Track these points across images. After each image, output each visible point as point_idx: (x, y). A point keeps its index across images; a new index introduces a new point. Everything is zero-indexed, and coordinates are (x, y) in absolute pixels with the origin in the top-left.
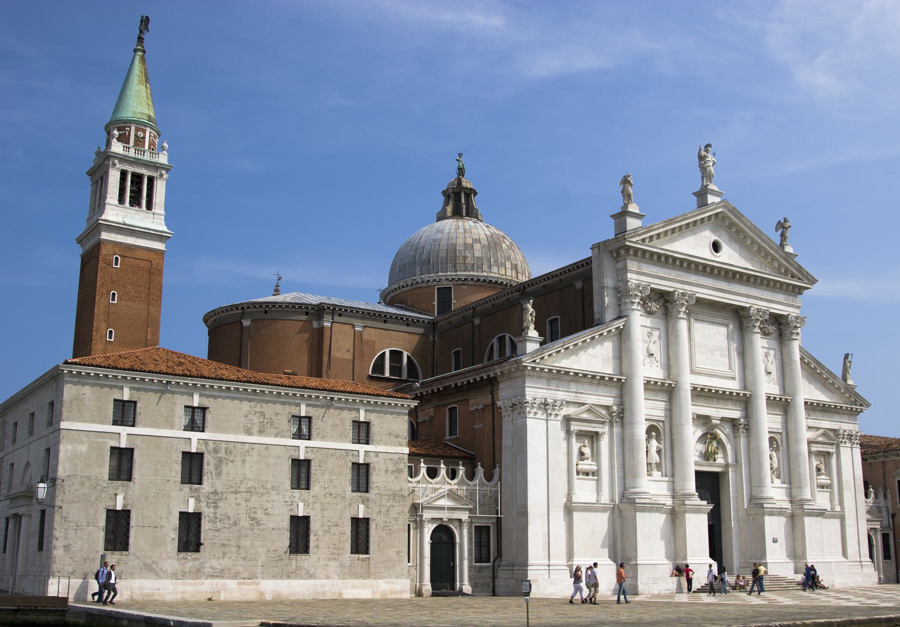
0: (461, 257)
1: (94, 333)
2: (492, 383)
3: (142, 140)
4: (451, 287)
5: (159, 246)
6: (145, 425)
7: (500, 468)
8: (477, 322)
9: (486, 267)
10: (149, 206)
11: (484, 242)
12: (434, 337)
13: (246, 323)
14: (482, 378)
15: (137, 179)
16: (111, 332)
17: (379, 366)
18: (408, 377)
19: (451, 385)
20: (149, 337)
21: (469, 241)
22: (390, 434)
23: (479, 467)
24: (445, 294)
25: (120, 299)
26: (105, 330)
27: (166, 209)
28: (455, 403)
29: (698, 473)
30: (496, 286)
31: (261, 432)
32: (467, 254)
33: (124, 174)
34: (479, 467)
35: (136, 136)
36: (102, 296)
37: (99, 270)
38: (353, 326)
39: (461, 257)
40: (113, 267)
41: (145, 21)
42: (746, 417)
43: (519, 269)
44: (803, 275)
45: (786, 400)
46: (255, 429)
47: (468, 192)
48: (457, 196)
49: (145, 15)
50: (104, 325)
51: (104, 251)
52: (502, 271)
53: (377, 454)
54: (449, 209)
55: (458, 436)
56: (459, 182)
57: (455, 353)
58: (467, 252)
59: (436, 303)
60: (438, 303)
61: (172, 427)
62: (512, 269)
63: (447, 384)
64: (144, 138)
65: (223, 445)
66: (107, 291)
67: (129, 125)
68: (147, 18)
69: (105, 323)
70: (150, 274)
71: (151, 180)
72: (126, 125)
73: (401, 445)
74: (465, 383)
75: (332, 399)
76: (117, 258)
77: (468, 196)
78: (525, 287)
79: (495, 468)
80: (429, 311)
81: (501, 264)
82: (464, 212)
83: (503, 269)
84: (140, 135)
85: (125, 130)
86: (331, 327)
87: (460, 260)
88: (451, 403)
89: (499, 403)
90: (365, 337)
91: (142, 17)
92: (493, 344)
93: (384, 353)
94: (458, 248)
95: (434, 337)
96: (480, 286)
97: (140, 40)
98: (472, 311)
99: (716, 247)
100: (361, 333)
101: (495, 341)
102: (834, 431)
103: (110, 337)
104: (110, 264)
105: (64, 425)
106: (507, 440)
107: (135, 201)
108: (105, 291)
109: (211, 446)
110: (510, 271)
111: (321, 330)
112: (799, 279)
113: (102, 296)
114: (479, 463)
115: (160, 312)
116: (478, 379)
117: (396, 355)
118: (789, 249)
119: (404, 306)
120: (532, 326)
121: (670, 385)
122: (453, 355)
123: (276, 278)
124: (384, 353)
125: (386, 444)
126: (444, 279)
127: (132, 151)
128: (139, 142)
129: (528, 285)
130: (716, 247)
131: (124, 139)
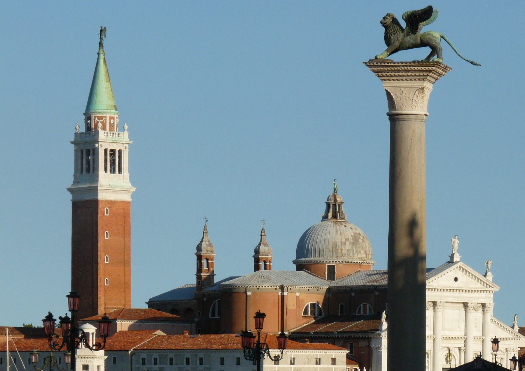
0: (339, 249)
1: (99, 259)
2: (369, 339)
3: (113, 125)
4: (334, 265)
5: (127, 198)
6: (282, 364)
7: (372, 369)
8: (353, 294)
9: (352, 255)
10: (120, 171)
11: (351, 240)
12: (329, 295)
13: (249, 293)
14: (365, 336)
15: (113, 151)
16: (107, 257)
17: (306, 312)
18: (318, 315)
19: (352, 336)
20: (126, 258)
21: (344, 241)
22: (341, 362)
23: (365, 369)
24: (331, 269)
25: (110, 236)
26: (104, 257)
27: (130, 172)
28: (353, 342)
29: (442, 368)
30: (357, 264)
31: (308, 364)
32: (343, 248)
33: (106, 151)
34: (365, 369)
35: (110, 123)
36: (101, 235)
37: (99, 219)
38: (296, 293)
39: (339, 249)
40: (105, 216)
41: (102, 31)
42: (465, 346)
43: (367, 253)
44: (494, 286)
45: (483, 338)
46: (306, 363)
47: (340, 204)
48: (335, 205)
49: (104, 26)
50: (103, 254)
51: (100, 206)
52: (359, 256)
53: (338, 368)
54: (330, 215)
55: (354, 354)
56: (335, 197)
57: (341, 305)
58: (342, 247)
59: (326, 273)
60: (328, 272)
61: (287, 364)
62: (364, 254)
63: (350, 335)
64: (114, 123)
65: (299, 369)
66: (104, 231)
67: (105, 115)
68: (105, 28)
69: (104, 252)
70: (124, 217)
71: (120, 151)
72: (103, 115)
73: (344, 365)
74: (358, 336)
75: (326, 352)
76: (107, 209)
77: (339, 206)
78: (377, 287)
79: (369, 368)
80: (323, 277)
81: (359, 252)
82: (338, 217)
83: (360, 254)
84: (112, 121)
85: (103, 119)
86: (287, 295)
87: (339, 251)
88: (350, 342)
89: (371, 346)
90: (300, 298)
91: (101, 28)
92: (360, 307)
93: (308, 305)
94: (338, 245)
95: (329, 295)
96: (349, 265)
97: (101, 44)
98: (350, 288)
99: (456, 279)
100: (299, 296)
101: (362, 305)
102: (506, 349)
103: (107, 261)
104: (104, 214)
105: (264, 365)
106: (374, 359)
107: (113, 171)
108: (102, 232)
109: (296, 369)
110: (363, 254)
111: (282, 297)
112: (492, 288)
113: (101, 235)
114: (365, 367)
115: (130, 242)
116: (364, 336)
117: (313, 305)
118: (489, 274)
119: (310, 272)
120: (385, 320)
121: (433, 337)
122: (339, 306)
123: (205, 221)
124: (308, 305)
125: (340, 365)
126: (331, 261)
127: (109, 134)
128: (112, 127)
129: (379, 286)
130: (456, 279)
131: (104, 128)
